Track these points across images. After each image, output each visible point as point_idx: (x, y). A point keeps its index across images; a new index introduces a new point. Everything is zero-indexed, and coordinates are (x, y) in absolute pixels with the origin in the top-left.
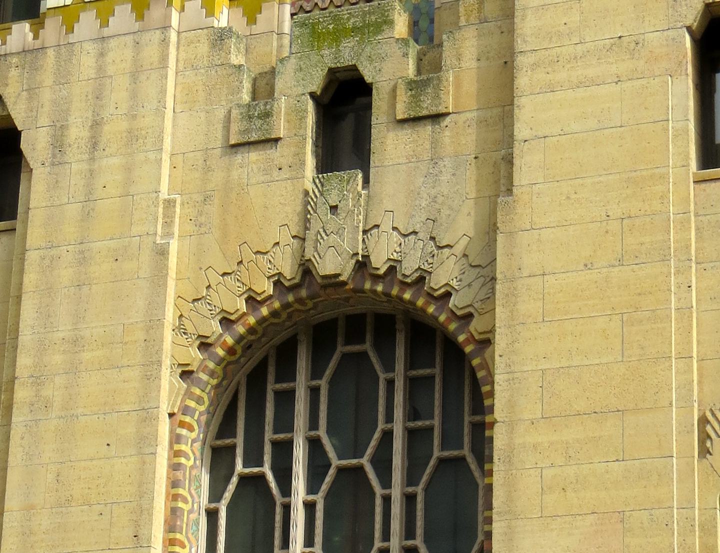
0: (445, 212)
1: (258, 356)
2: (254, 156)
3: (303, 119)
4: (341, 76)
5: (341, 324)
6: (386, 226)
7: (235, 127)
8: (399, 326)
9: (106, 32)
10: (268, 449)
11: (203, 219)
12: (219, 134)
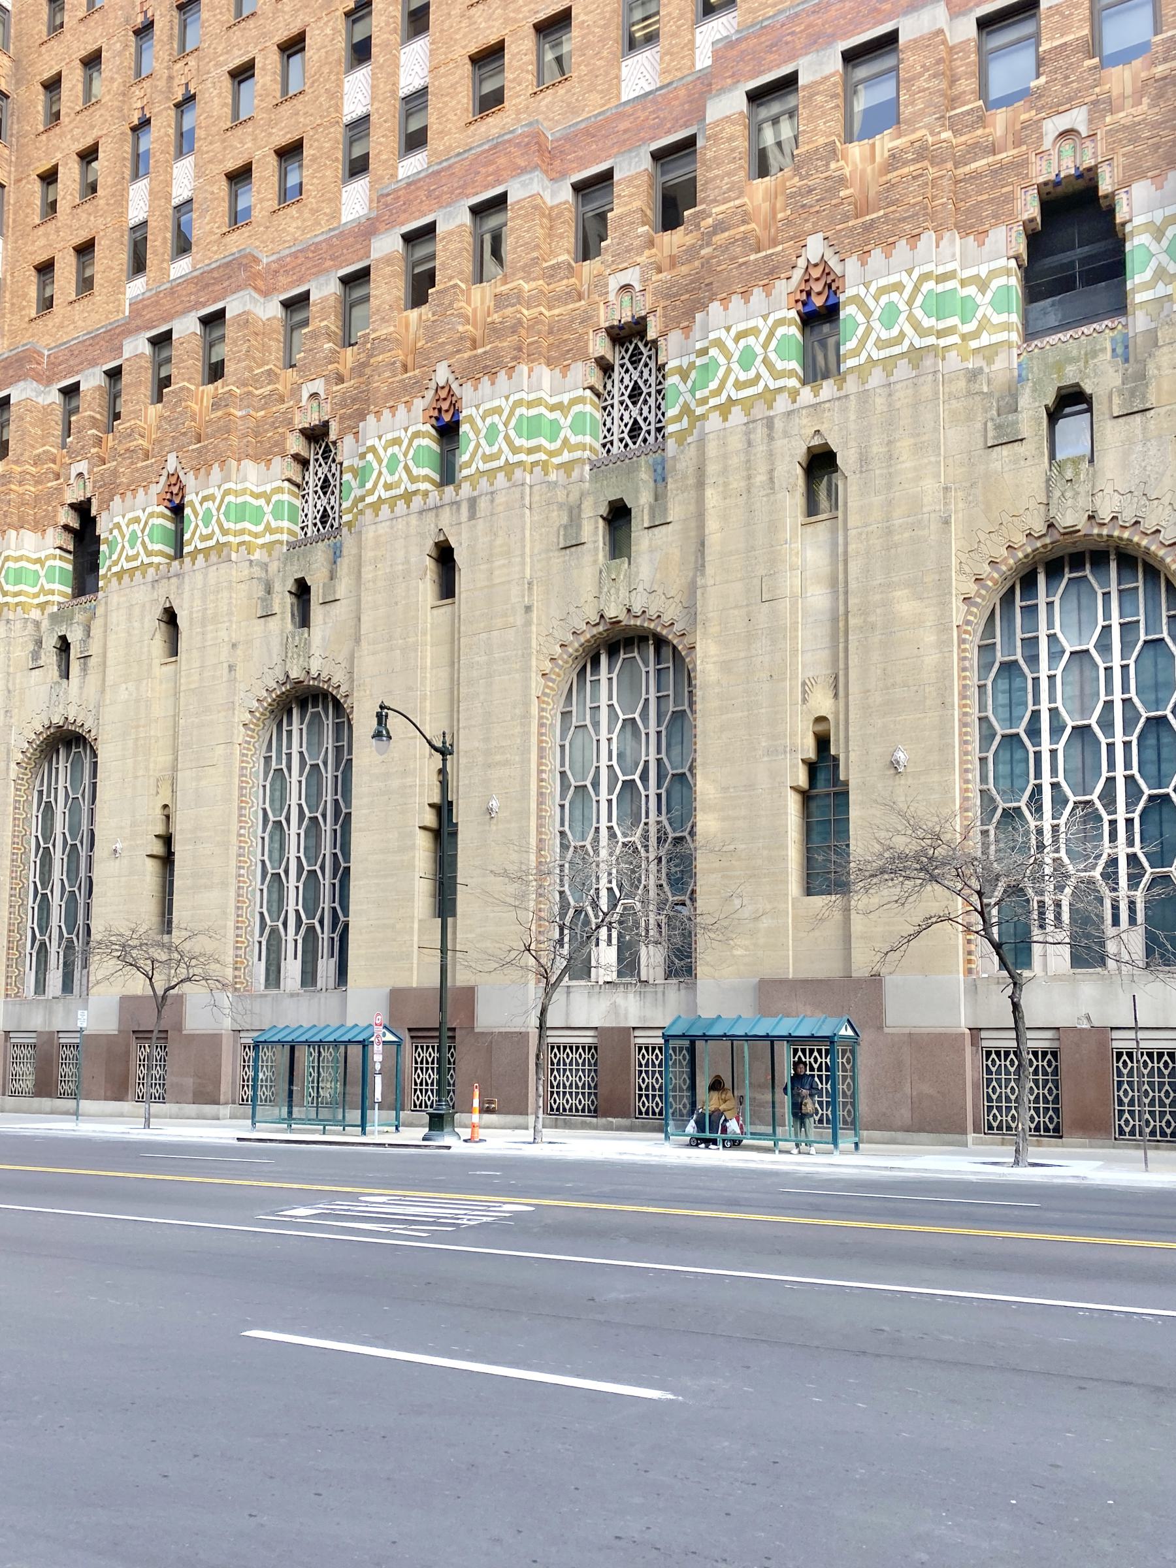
0: (1153, 476)
1: (1011, 583)
2: (1005, 451)
3: (1040, 424)
4: (1064, 392)
5: (1067, 559)
6: (1109, 490)
7: (991, 434)
8: (1112, 557)
9: (892, 379)
10: (1019, 643)
11: (971, 498)
12: (980, 441)
